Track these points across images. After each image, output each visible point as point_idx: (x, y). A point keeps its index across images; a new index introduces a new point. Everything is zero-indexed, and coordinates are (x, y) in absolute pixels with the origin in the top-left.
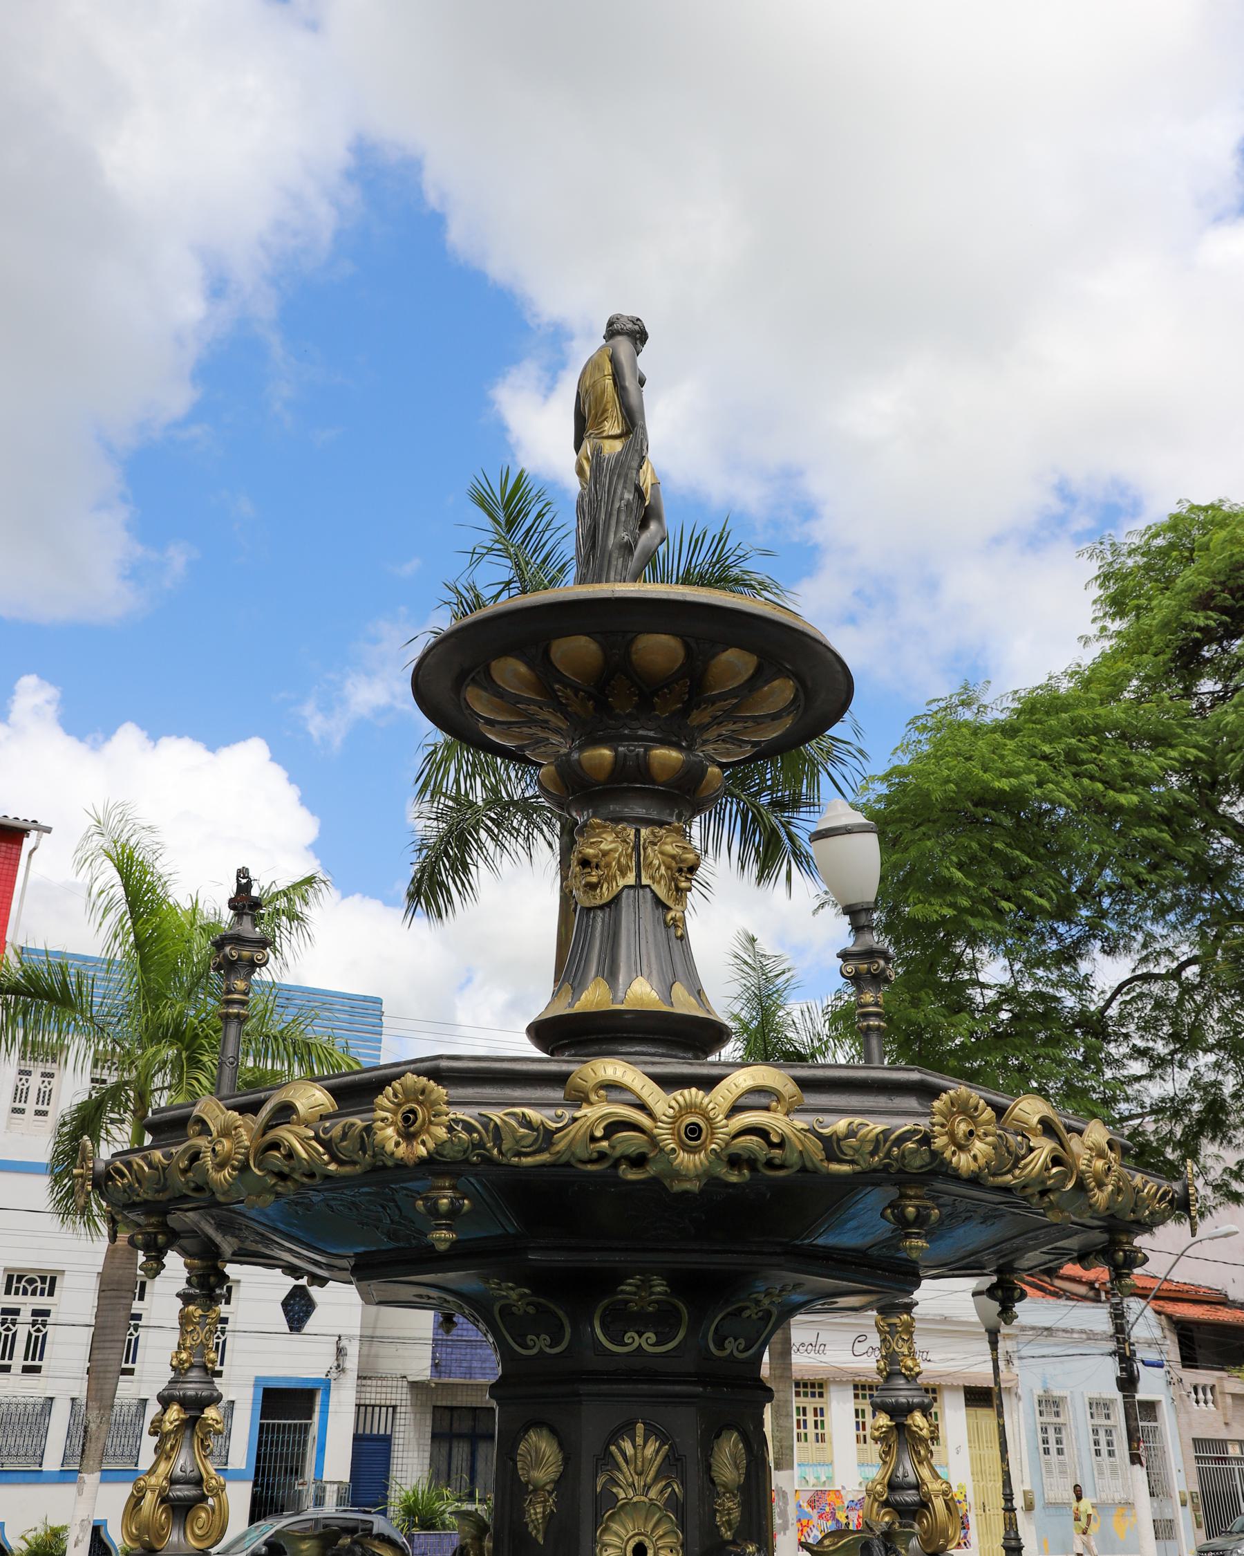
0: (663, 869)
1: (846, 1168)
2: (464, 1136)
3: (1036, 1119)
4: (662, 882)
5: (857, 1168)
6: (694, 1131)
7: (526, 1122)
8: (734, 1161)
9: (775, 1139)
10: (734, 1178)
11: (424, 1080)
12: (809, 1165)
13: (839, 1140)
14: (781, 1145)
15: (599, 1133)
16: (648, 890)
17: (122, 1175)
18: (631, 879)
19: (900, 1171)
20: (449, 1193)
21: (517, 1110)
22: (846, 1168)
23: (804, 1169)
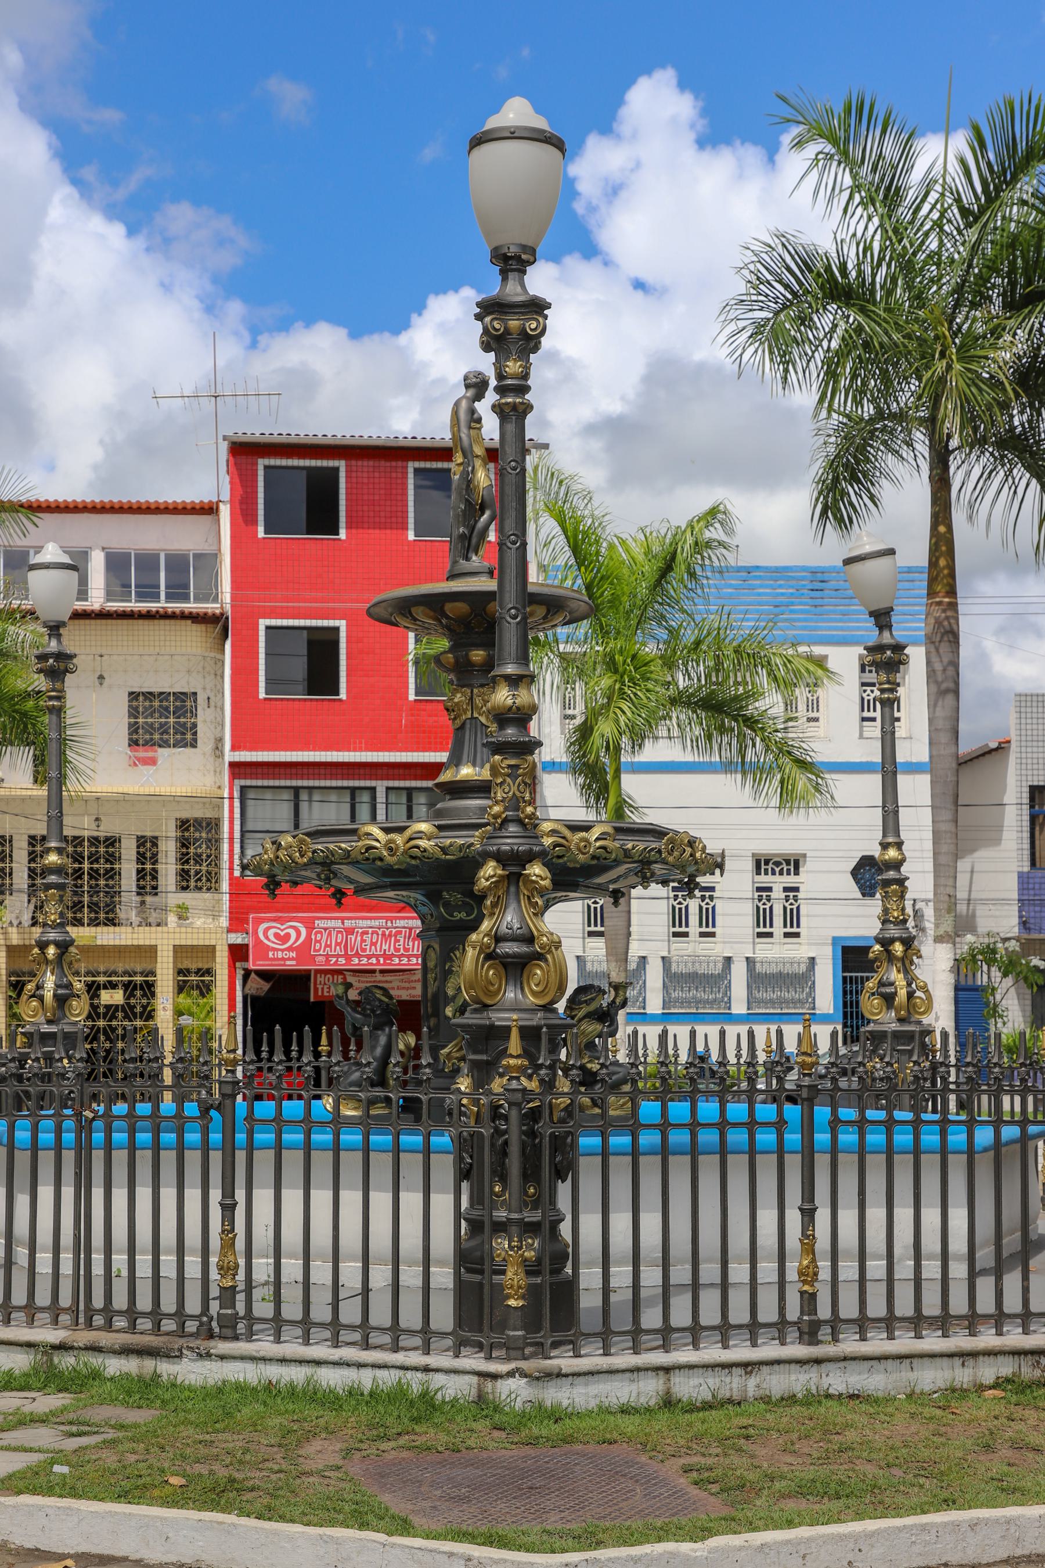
6: (391, 849)
8: (412, 857)
10: (413, 862)
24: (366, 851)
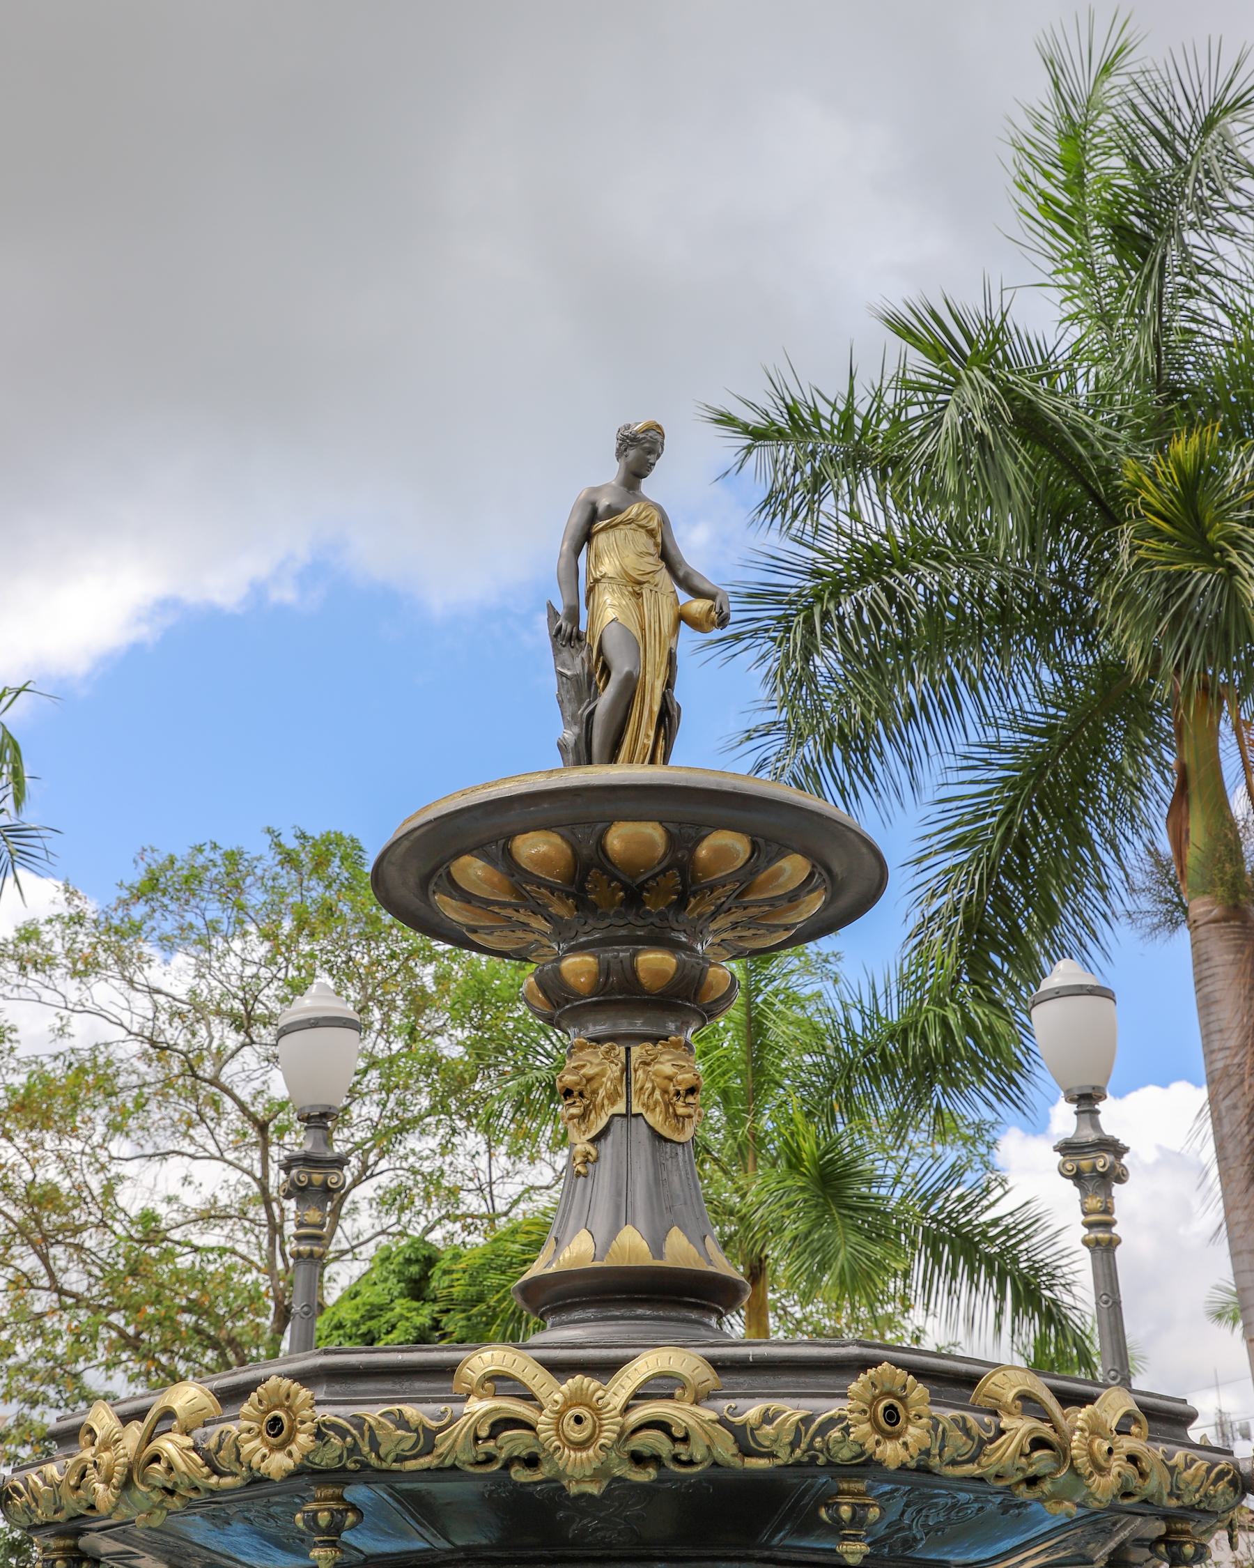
0: (657, 1094)
1: (762, 1463)
2: (336, 1441)
3: (1011, 1395)
4: (658, 1110)
5: (779, 1462)
7: (402, 1422)
8: (638, 1459)
9: (678, 1433)
11: (287, 1382)
12: (719, 1460)
13: (752, 1429)
14: (685, 1440)
15: (484, 1433)
16: (640, 1119)
17: (20, 1495)
18: (620, 1108)
19: (829, 1464)
20: (333, 1505)
21: (395, 1407)
22: (762, 1463)
23: (715, 1464)
24: (492, 1436)
